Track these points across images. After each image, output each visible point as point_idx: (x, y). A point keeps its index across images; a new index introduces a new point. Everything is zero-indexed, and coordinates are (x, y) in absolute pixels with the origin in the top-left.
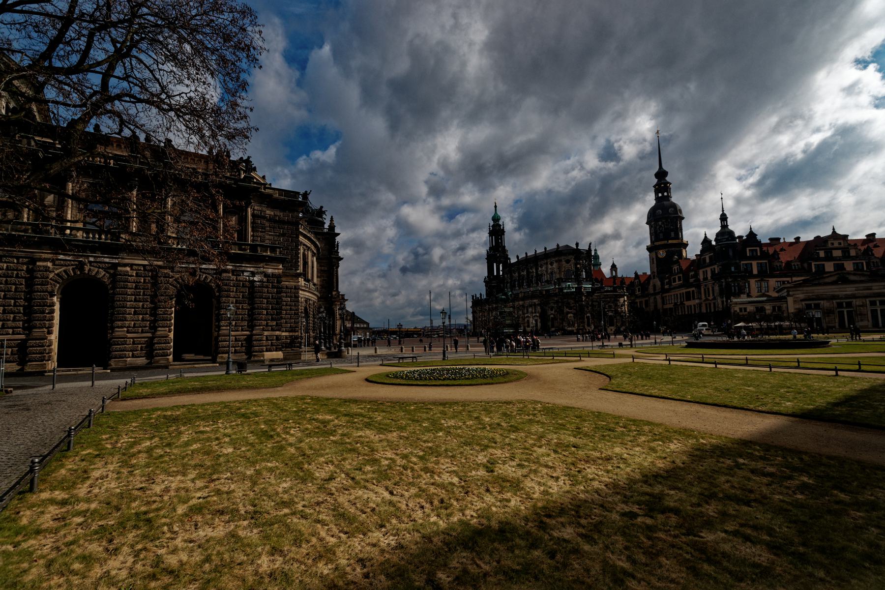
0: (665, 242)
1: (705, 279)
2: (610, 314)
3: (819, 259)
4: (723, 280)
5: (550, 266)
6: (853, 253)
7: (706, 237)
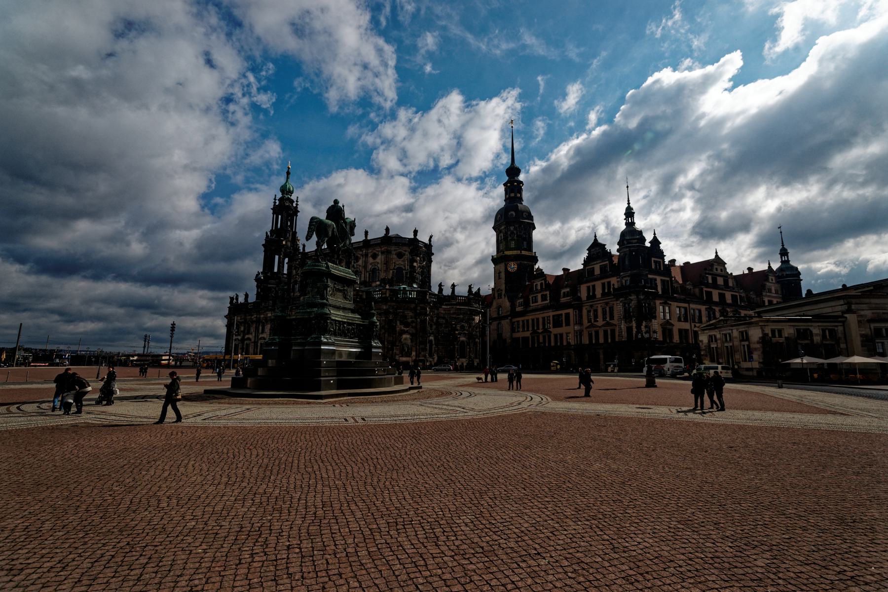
0: (519, 252)
1: (591, 297)
2: (463, 339)
3: (708, 285)
4: (633, 297)
5: (371, 260)
6: (731, 284)
7: (596, 240)
